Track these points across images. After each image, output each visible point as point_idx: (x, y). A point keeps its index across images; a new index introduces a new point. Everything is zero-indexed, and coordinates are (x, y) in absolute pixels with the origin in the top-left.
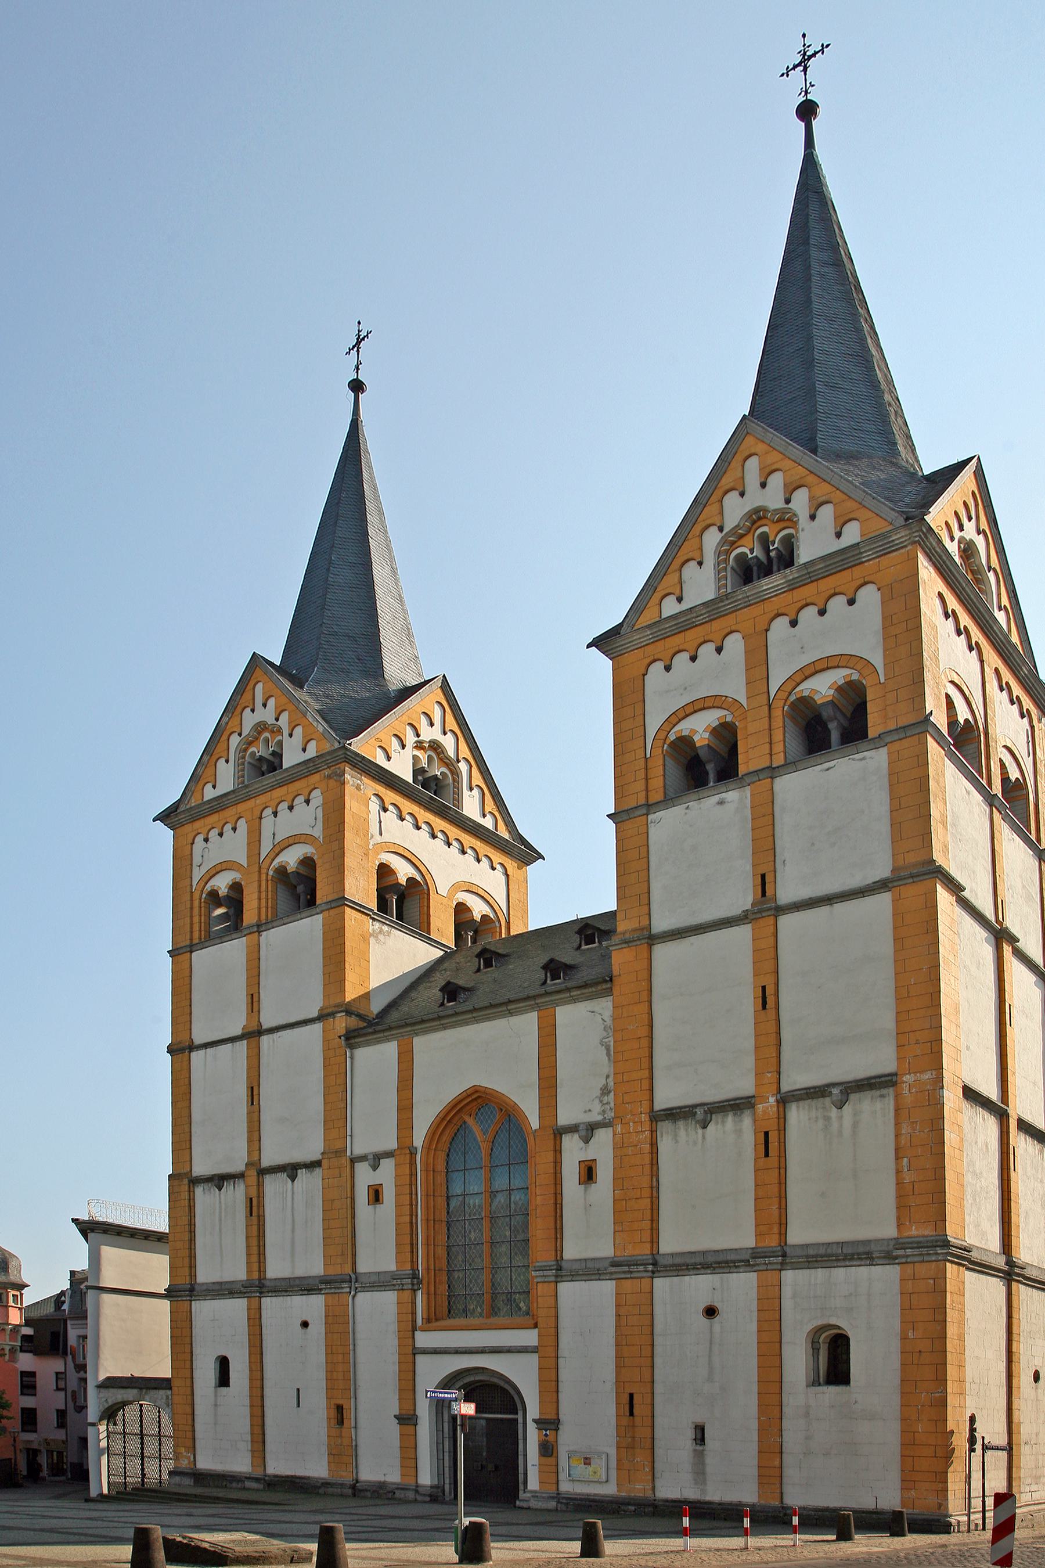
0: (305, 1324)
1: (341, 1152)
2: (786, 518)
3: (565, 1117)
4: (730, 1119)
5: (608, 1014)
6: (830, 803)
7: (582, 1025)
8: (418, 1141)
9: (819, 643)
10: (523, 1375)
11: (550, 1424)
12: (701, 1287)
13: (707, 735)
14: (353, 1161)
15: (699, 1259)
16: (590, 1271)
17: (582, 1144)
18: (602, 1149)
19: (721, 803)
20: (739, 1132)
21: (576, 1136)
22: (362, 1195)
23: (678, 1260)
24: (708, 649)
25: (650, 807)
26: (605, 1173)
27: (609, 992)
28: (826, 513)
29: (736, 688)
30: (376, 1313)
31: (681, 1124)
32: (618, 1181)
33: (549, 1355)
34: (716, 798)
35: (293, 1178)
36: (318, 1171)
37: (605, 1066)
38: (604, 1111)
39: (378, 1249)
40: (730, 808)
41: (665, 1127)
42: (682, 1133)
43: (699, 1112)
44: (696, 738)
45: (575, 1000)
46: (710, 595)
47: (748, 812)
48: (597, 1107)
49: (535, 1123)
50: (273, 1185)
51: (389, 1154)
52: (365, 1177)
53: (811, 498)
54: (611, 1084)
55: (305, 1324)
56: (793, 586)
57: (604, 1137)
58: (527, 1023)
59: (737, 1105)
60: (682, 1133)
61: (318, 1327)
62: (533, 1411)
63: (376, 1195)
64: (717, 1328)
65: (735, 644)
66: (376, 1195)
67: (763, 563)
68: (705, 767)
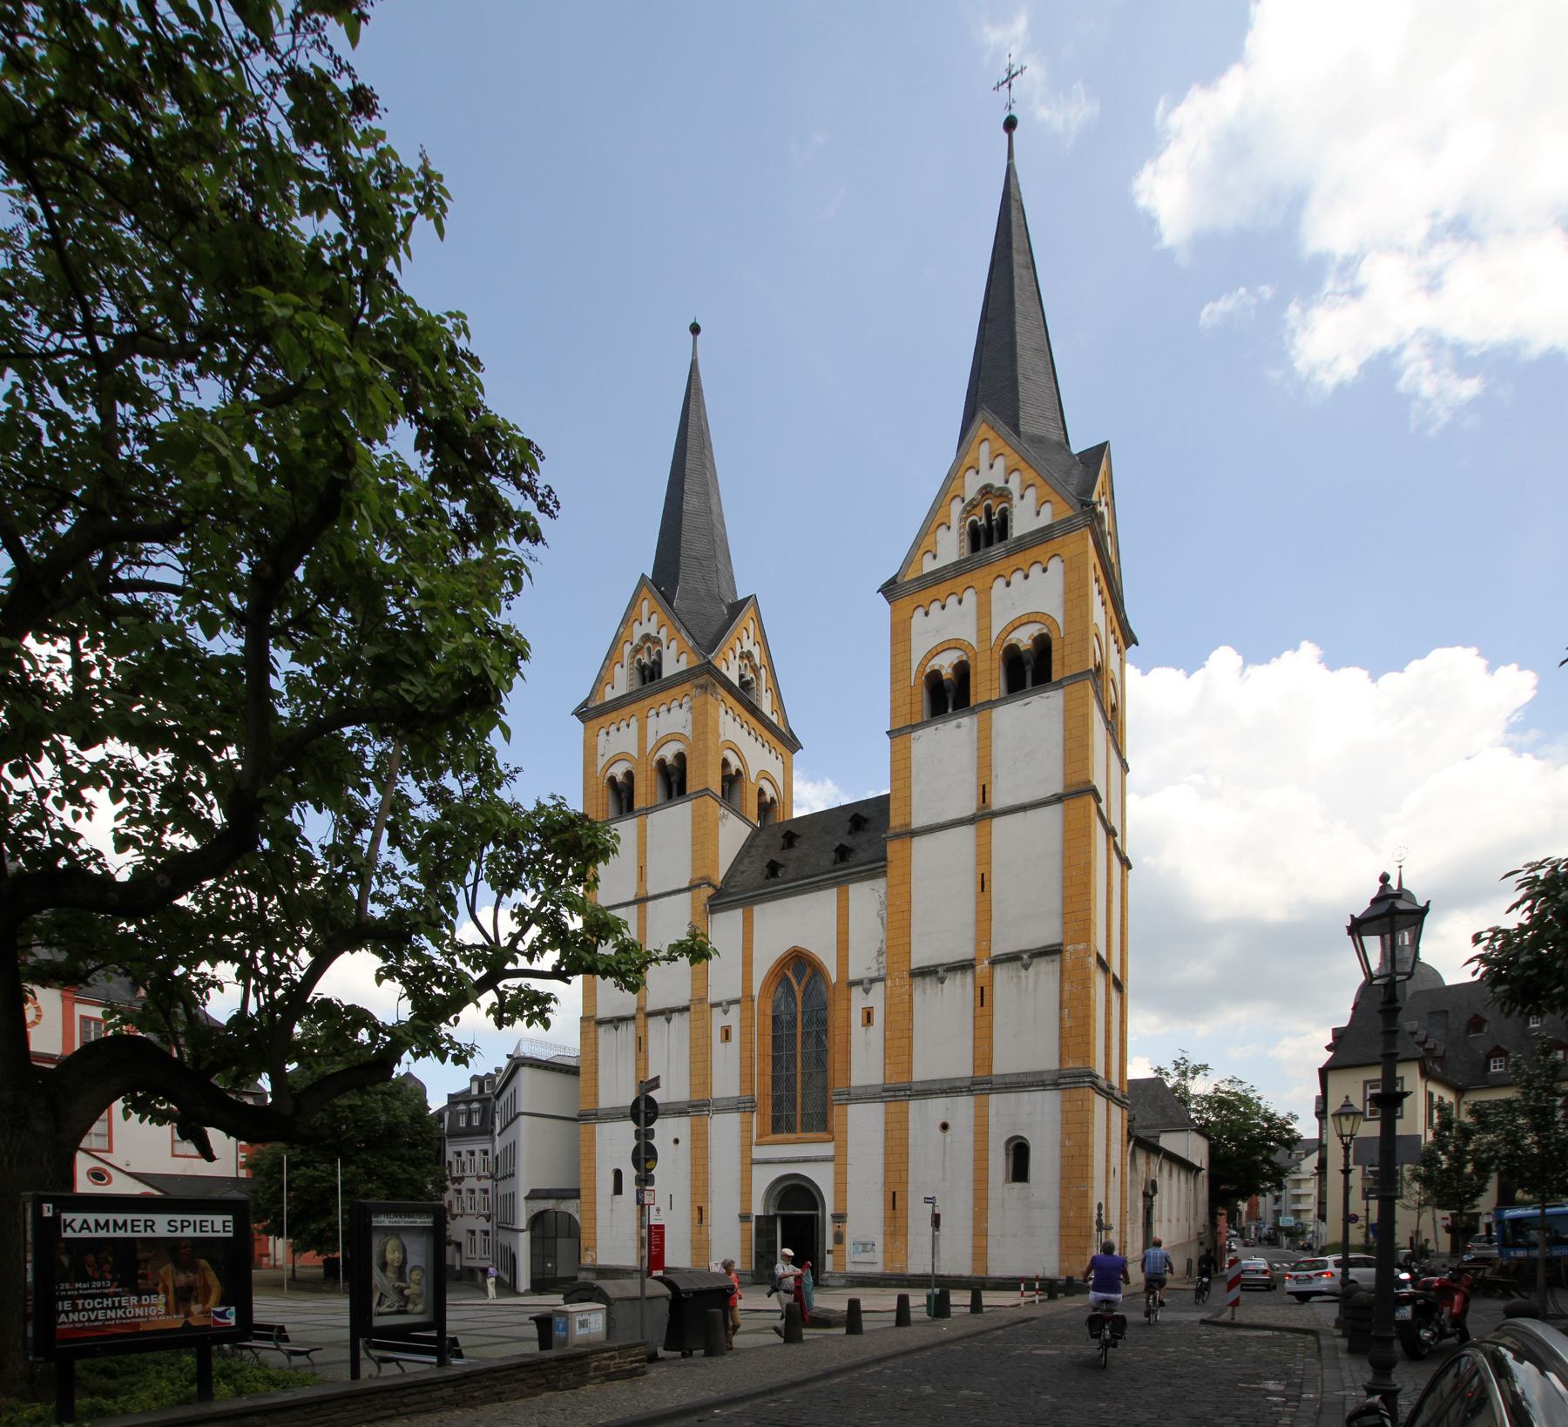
0: (676, 1141)
1: (703, 1000)
2: (1004, 495)
3: (853, 976)
4: (959, 976)
5: (882, 892)
6: (1029, 724)
7: (866, 897)
8: (756, 992)
9: (1028, 598)
10: (821, 1176)
11: (840, 1218)
12: (937, 1108)
14: (713, 1006)
15: (938, 1086)
16: (867, 1096)
18: (876, 998)
19: (958, 726)
20: (964, 986)
21: (860, 988)
22: (717, 1034)
23: (925, 1087)
24: (952, 600)
25: (914, 727)
26: (878, 1017)
27: (884, 874)
28: (1031, 494)
29: (969, 634)
30: (725, 1130)
31: (928, 980)
32: (887, 1023)
33: (839, 1161)
34: (954, 723)
35: (669, 1021)
36: (687, 1014)
37: (880, 934)
39: (726, 1080)
40: (964, 730)
41: (918, 981)
42: (928, 986)
43: (940, 970)
45: (862, 879)
46: (955, 558)
47: (975, 735)
48: (875, 966)
49: (834, 978)
50: (655, 1024)
51: (737, 1002)
52: (718, 1020)
53: (1022, 481)
55: (676, 1141)
56: (1010, 553)
57: (878, 988)
58: (829, 897)
59: (965, 966)
60: (928, 986)
61: (685, 1143)
62: (830, 1209)
63: (727, 1034)
64: (948, 1140)
65: (970, 597)
66: (727, 1034)
67: (988, 532)
68: (947, 695)
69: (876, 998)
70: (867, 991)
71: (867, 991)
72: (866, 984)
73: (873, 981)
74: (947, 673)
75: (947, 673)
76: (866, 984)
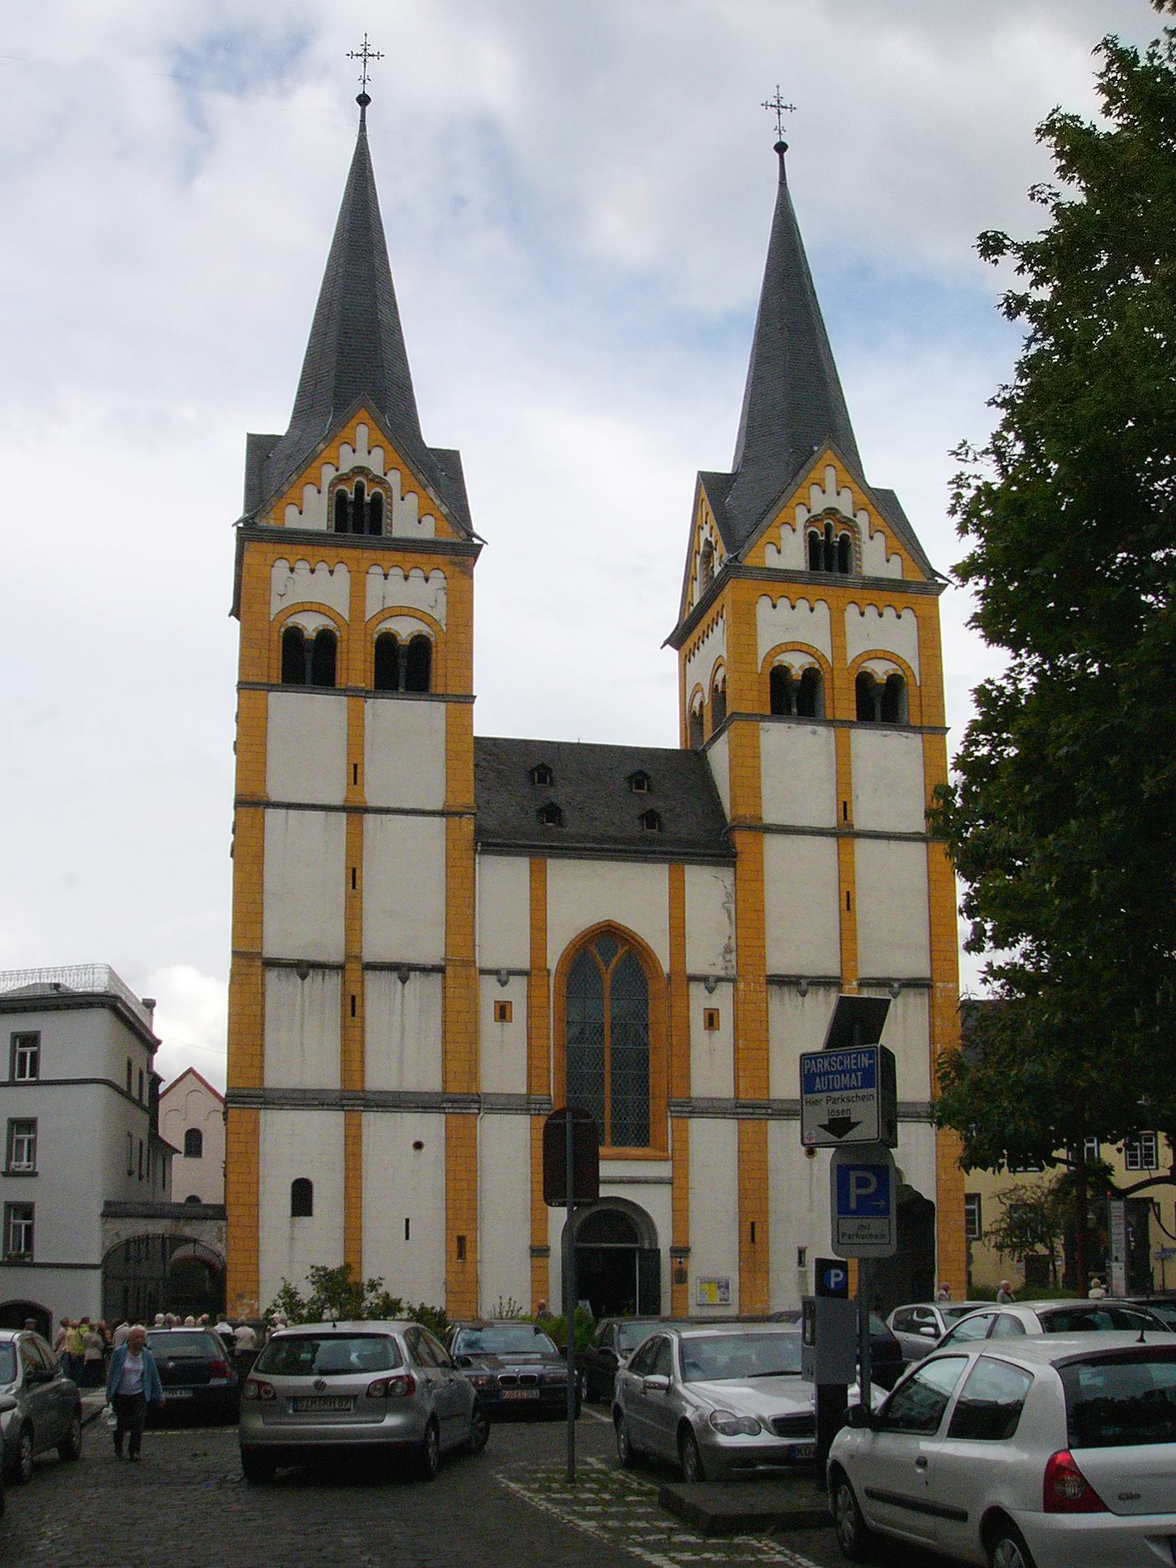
4: (821, 991)
13: (801, 673)
17: (707, 993)
19: (814, 733)
21: (702, 985)
31: (785, 989)
34: (809, 728)
38: (726, 968)
41: (774, 988)
42: (787, 998)
44: (793, 672)
47: (833, 747)
48: (720, 962)
49: (666, 967)
54: (733, 945)
57: (726, 989)
60: (787, 998)
69: (723, 1000)
70: (711, 990)
71: (711, 990)
72: (710, 983)
73: (719, 979)
74: (797, 673)
75: (797, 673)
76: (710, 983)
